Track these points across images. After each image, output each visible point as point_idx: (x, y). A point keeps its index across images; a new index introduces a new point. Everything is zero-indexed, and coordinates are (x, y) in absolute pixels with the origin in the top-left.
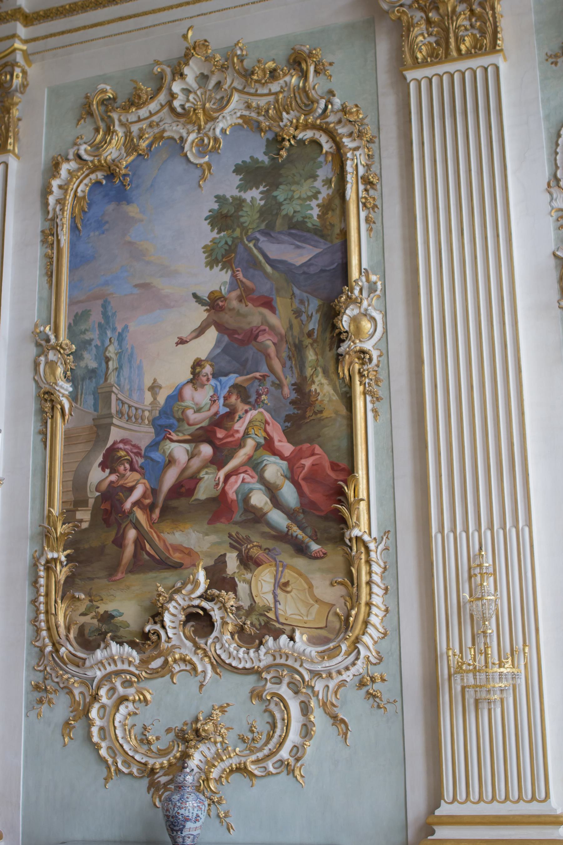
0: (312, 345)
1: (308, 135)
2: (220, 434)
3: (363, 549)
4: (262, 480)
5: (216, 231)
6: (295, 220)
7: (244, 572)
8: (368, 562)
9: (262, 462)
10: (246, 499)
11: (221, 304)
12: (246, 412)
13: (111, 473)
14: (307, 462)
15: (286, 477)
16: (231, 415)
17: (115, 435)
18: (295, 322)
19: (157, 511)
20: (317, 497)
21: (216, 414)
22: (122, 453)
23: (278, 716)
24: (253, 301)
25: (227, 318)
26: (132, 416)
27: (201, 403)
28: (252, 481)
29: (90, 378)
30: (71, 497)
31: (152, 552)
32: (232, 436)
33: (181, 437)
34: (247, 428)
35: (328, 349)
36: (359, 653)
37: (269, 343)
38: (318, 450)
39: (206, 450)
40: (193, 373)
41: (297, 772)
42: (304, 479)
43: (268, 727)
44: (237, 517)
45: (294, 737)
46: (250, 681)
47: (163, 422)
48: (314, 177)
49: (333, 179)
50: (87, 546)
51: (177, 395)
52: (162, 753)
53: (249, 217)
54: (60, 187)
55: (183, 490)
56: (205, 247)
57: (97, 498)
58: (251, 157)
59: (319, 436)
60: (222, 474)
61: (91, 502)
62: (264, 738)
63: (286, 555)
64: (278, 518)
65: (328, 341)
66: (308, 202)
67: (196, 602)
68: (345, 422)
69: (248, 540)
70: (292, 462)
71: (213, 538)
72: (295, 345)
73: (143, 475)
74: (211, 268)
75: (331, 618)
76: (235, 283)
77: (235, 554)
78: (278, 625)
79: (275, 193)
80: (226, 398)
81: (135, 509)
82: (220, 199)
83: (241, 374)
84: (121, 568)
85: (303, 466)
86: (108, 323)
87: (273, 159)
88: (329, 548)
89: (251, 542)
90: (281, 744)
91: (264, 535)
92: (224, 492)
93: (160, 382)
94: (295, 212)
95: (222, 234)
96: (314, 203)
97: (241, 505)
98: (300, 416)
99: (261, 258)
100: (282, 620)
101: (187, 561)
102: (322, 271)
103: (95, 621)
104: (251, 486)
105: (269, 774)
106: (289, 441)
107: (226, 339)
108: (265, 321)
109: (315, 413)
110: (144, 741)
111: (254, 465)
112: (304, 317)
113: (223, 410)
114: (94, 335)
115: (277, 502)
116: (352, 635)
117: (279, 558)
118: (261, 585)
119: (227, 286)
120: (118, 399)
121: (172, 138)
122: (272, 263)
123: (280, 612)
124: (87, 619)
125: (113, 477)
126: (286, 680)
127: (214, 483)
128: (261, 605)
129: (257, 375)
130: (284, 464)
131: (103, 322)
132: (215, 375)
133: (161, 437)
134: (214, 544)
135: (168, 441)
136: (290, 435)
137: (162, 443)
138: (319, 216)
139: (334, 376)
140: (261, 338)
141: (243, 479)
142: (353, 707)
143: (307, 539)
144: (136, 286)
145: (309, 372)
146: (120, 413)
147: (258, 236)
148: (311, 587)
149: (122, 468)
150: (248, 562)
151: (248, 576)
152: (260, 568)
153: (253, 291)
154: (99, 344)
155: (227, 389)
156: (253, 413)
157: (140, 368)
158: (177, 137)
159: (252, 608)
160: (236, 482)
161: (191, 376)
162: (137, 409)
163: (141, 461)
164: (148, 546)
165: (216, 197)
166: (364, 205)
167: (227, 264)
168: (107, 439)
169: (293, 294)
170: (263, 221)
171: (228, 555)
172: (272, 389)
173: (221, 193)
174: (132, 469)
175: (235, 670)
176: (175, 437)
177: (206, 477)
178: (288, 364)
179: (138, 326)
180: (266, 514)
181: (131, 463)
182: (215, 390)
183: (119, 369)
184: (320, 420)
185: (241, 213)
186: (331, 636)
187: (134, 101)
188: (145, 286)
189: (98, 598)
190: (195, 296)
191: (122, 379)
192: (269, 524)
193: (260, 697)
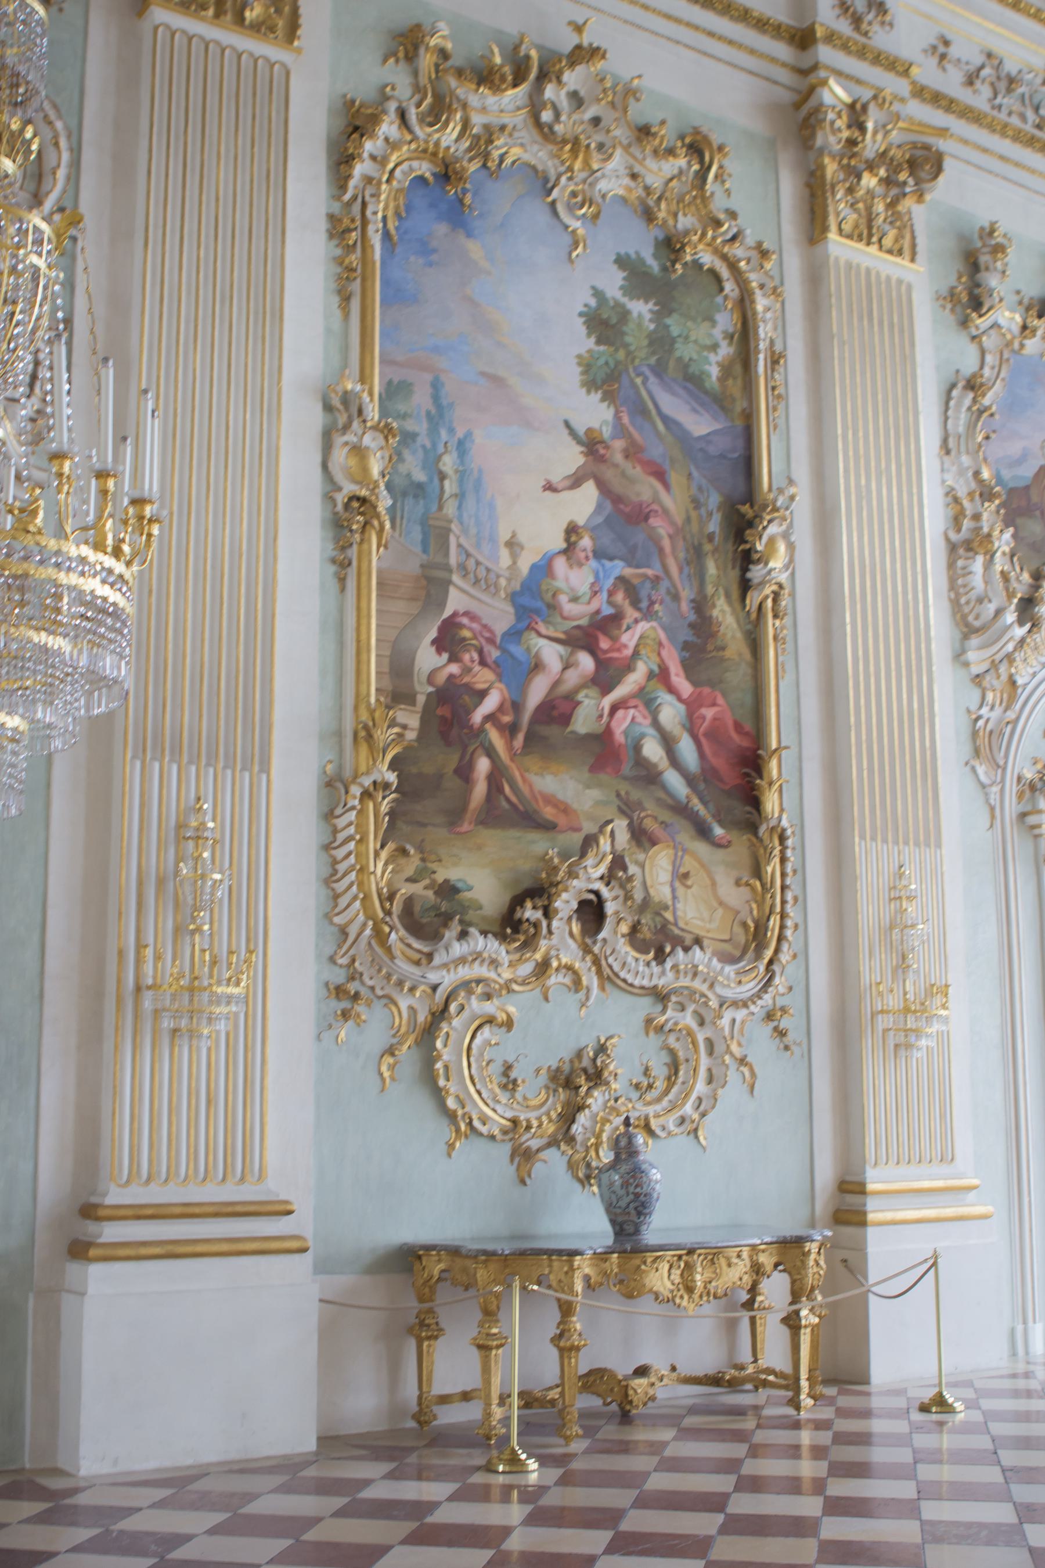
1: (707, 259)
2: (604, 644)
3: (776, 842)
4: (656, 724)
5: (593, 339)
7: (635, 849)
8: (783, 860)
9: (656, 698)
10: (637, 748)
11: (602, 451)
12: (636, 621)
13: (451, 660)
14: (709, 713)
15: (684, 726)
16: (616, 618)
17: (455, 602)
18: (694, 514)
19: (520, 738)
20: (720, 763)
21: (598, 612)
22: (466, 633)
23: (681, 1054)
25: (609, 474)
26: (485, 581)
27: (579, 588)
29: (416, 496)
30: (387, 684)
31: (514, 799)
32: (619, 650)
34: (637, 646)
35: (730, 566)
37: (662, 532)
38: (720, 700)
39: (586, 662)
40: (567, 540)
41: (700, 1133)
42: (705, 735)
44: (627, 769)
45: (701, 1087)
46: (645, 1006)
47: (526, 601)
48: (714, 323)
49: (736, 336)
50: (414, 770)
51: (544, 568)
53: (635, 339)
55: (555, 713)
56: (579, 356)
57: (429, 695)
58: (637, 253)
59: (721, 682)
60: (607, 702)
61: (421, 699)
62: (660, 1084)
63: (686, 836)
64: (674, 780)
66: (705, 353)
68: (750, 671)
70: (692, 706)
71: (595, 794)
72: (694, 548)
73: (500, 677)
74: (589, 392)
76: (620, 429)
78: (677, 931)
79: (668, 321)
80: (611, 593)
81: (488, 726)
82: (598, 293)
83: (630, 565)
84: (468, 815)
85: (704, 718)
86: (441, 416)
87: (664, 269)
88: (734, 836)
89: (643, 809)
91: (659, 802)
93: (522, 538)
94: (690, 359)
95: (602, 348)
96: (713, 358)
97: (631, 753)
98: (699, 646)
99: (651, 406)
100: (681, 924)
101: (562, 821)
102: (722, 456)
103: (430, 893)
107: (609, 506)
108: (656, 499)
110: (510, 1085)
112: (703, 511)
113: (608, 611)
114: (419, 426)
116: (769, 953)
118: (656, 871)
119: (610, 428)
120: (459, 546)
121: (534, 168)
122: (666, 419)
123: (679, 913)
124: (417, 888)
125: (454, 669)
127: (598, 714)
128: (657, 899)
129: (649, 572)
130: (682, 708)
131: (433, 412)
133: (525, 624)
134: (598, 803)
135: (533, 635)
136: (689, 668)
137: (526, 634)
138: (719, 379)
139: (737, 605)
140: (653, 521)
143: (709, 819)
144: (483, 374)
145: (710, 589)
146: (462, 568)
148: (714, 884)
149: (466, 657)
150: (641, 837)
151: (641, 857)
152: (656, 848)
154: (428, 445)
156: (643, 626)
157: (492, 506)
158: (540, 168)
160: (624, 718)
161: (564, 545)
162: (488, 570)
164: (507, 789)
165: (593, 288)
167: (609, 397)
168: (442, 605)
169: (690, 474)
170: (653, 353)
172: (668, 599)
173: (600, 285)
174: (483, 663)
176: (543, 629)
177: (586, 701)
178: (686, 570)
179: (490, 442)
180: (661, 773)
181: (481, 652)
182: (597, 575)
183: (460, 496)
185: (625, 328)
187: (485, 77)
188: (496, 380)
189: (433, 857)
190: (567, 424)
191: (465, 515)
192: (664, 788)
193: (660, 1029)
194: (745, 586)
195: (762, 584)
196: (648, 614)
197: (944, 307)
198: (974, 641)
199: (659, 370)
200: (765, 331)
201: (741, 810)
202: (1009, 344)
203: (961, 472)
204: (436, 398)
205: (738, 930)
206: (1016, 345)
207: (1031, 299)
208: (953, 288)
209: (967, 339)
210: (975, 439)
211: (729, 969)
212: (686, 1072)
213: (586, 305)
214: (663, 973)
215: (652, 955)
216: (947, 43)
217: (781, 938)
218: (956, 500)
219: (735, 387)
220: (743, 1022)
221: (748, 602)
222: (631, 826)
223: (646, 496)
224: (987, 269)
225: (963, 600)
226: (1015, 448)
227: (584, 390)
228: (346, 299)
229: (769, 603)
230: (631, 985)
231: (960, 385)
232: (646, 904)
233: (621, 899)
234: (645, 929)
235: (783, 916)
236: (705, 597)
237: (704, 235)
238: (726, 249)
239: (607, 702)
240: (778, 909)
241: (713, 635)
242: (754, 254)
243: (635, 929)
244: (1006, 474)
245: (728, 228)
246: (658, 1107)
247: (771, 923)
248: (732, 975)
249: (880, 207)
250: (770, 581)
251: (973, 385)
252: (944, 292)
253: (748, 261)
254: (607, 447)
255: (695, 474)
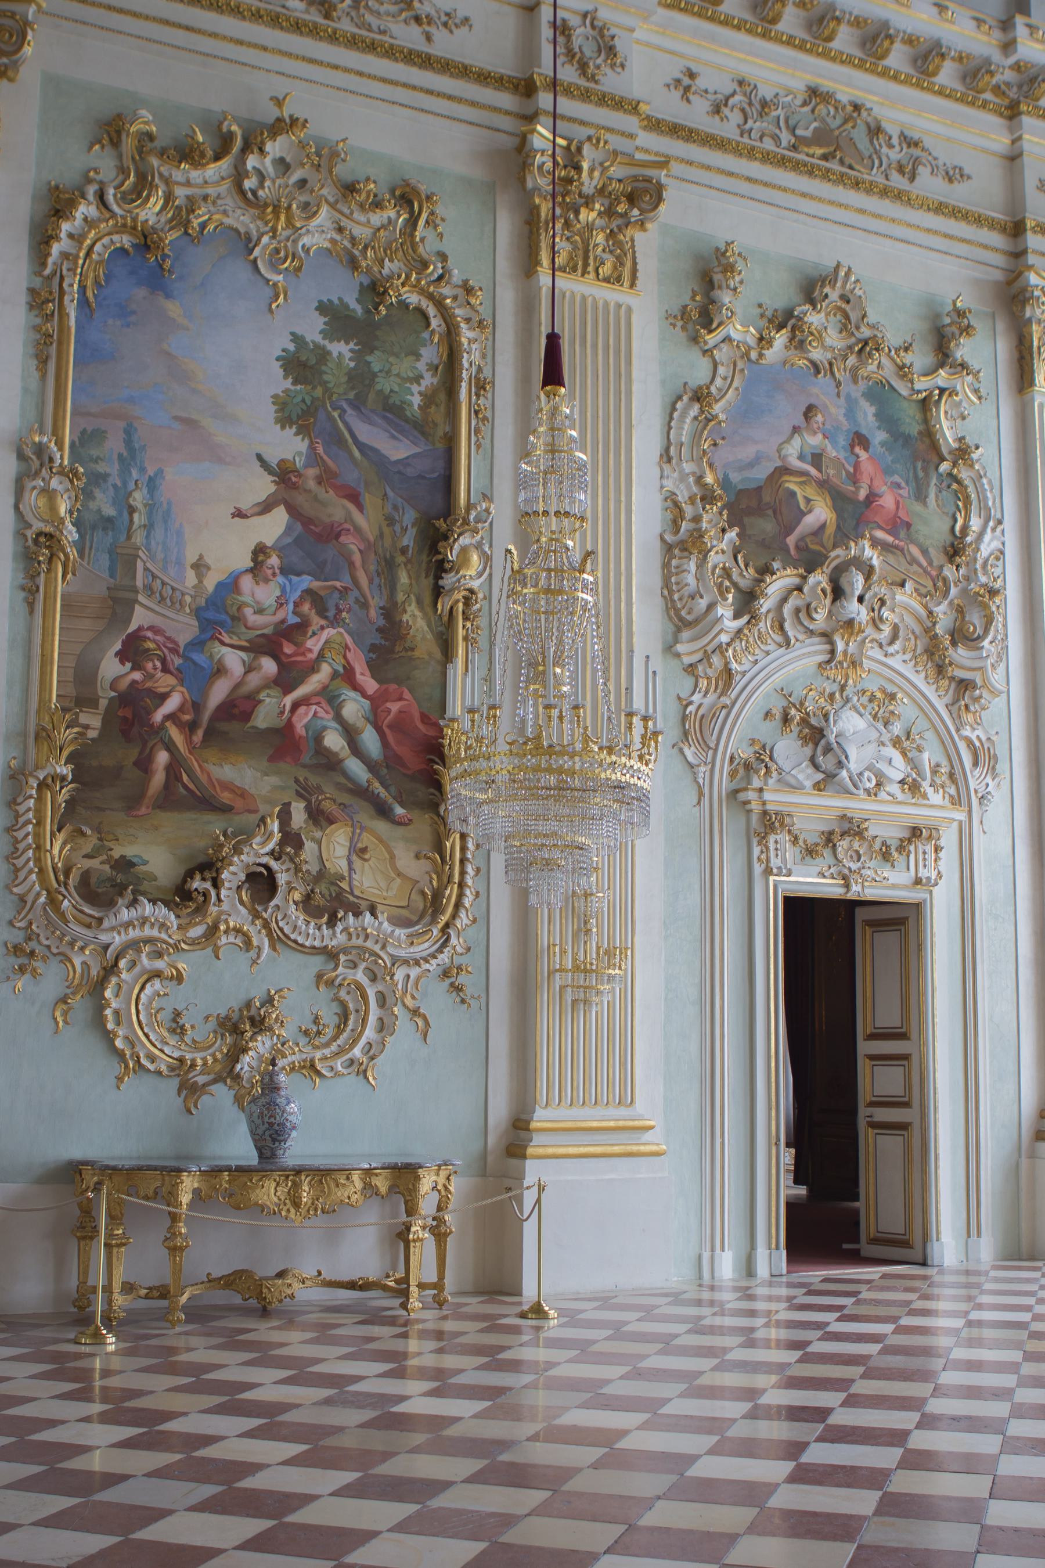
0: (405, 565)
1: (413, 299)
2: (288, 649)
4: (339, 718)
5: (290, 380)
6: (391, 401)
9: (340, 695)
10: (318, 739)
11: (294, 479)
12: (322, 628)
13: (133, 669)
14: (395, 707)
15: (367, 719)
16: (302, 626)
17: (140, 618)
18: (387, 531)
19: (200, 733)
20: (404, 751)
21: (283, 621)
22: (151, 645)
23: (351, 1006)
24: (337, 488)
26: (171, 599)
27: (264, 601)
28: (327, 718)
29: (105, 529)
30: (71, 690)
31: (191, 786)
32: (303, 654)
33: (235, 641)
34: (322, 649)
36: (448, 940)
37: (353, 547)
38: (407, 695)
39: (269, 666)
40: (254, 560)
41: (369, 1074)
42: (389, 726)
43: (336, 1019)
44: (306, 758)
45: (370, 1033)
46: (317, 963)
47: (210, 615)
48: (418, 357)
50: (94, 763)
51: (231, 585)
52: (196, 1046)
53: (334, 377)
54: (71, 236)
55: (236, 711)
56: (275, 396)
57: (111, 699)
59: (409, 678)
60: (288, 700)
61: (103, 703)
62: (329, 1032)
63: (365, 816)
64: (355, 767)
65: (424, 565)
67: (265, 860)
69: (319, 789)
70: (376, 702)
71: (273, 780)
72: (386, 560)
73: (181, 682)
74: (283, 427)
75: (414, 896)
76: (313, 457)
77: (302, 805)
78: (351, 898)
79: (369, 358)
80: (296, 605)
81: (168, 724)
82: (296, 338)
83: (318, 579)
84: (146, 801)
85: (389, 711)
88: (415, 815)
89: (323, 793)
90: (355, 1042)
91: (339, 786)
92: (289, 725)
93: (209, 560)
94: (392, 391)
95: (299, 387)
96: (415, 388)
97: (312, 744)
98: (387, 648)
100: (357, 893)
101: (239, 804)
102: (421, 477)
104: (325, 723)
105: (337, 1074)
106: (373, 677)
107: (299, 527)
108: (349, 518)
109: (406, 650)
110: (178, 1029)
111: (329, 697)
112: (397, 527)
113: (293, 620)
115: (356, 750)
116: (444, 919)
117: (356, 818)
118: (334, 847)
120: (146, 569)
121: (237, 231)
122: (361, 447)
123: (355, 883)
124: (94, 863)
125: (137, 676)
126: (363, 966)
128: (332, 871)
129: (338, 584)
130: (367, 703)
131: (125, 454)
132: (286, 571)
133: (209, 635)
135: (217, 643)
137: (209, 643)
139: (429, 610)
140: (343, 539)
141: (315, 713)
142: (436, 1000)
143: (390, 800)
144: (176, 418)
145: (400, 597)
147: (345, 406)
148: (393, 857)
149: (150, 665)
150: (318, 817)
151: (318, 834)
153: (335, 475)
154: (119, 484)
155: (299, 593)
156: (329, 632)
157: (179, 533)
158: (242, 230)
159: (321, 875)
160: (306, 714)
161: (252, 564)
162: (173, 589)
163: (178, 661)
164: (185, 777)
165: (292, 334)
166: (476, 412)
167: (303, 430)
168: (128, 621)
169: (386, 494)
170: (353, 388)
171: (294, 804)
172: (356, 607)
173: (299, 332)
174: (165, 670)
175: (300, 948)
176: (227, 640)
177: (268, 700)
178: (376, 581)
179: (179, 477)
180: (342, 761)
181: (163, 661)
183: (149, 527)
184: (411, 659)
185: (324, 368)
186: (415, 918)
188: (190, 423)
189: (111, 837)
190: (259, 457)
191: (153, 542)
192: (345, 774)
193: (330, 983)
194: (438, 592)
195: (452, 590)
196: (335, 621)
197: (674, 326)
198: (685, 635)
199: (358, 404)
200: (470, 359)
201: (423, 792)
202: (746, 355)
203: (683, 477)
204: (128, 443)
205: (416, 897)
206: (754, 355)
207: (776, 310)
208: (685, 307)
209: (700, 354)
210: (699, 445)
211: (401, 933)
212: (356, 1021)
213: (283, 350)
214: (334, 934)
215: (325, 919)
216: (692, 75)
217: (458, 905)
218: (676, 504)
219: (438, 414)
220: (418, 979)
221: (439, 607)
222: (308, 809)
223: (338, 515)
224: (720, 287)
225: (676, 597)
226: (747, 453)
227: (278, 426)
228: (43, 361)
229: (460, 606)
230: (302, 945)
231: (685, 398)
232: (321, 875)
233: (292, 871)
234: (318, 897)
235: (462, 885)
236: (395, 604)
237: (408, 277)
238: (432, 289)
239: (288, 700)
240: (456, 879)
241: (403, 638)
242: (460, 292)
243: (308, 898)
244: (735, 477)
245: (434, 270)
246: (327, 1052)
247: (448, 892)
248: (403, 937)
249: (600, 238)
250: (458, 588)
251: (700, 396)
252: (676, 310)
253: (455, 298)
254: (300, 475)
255: (391, 494)
